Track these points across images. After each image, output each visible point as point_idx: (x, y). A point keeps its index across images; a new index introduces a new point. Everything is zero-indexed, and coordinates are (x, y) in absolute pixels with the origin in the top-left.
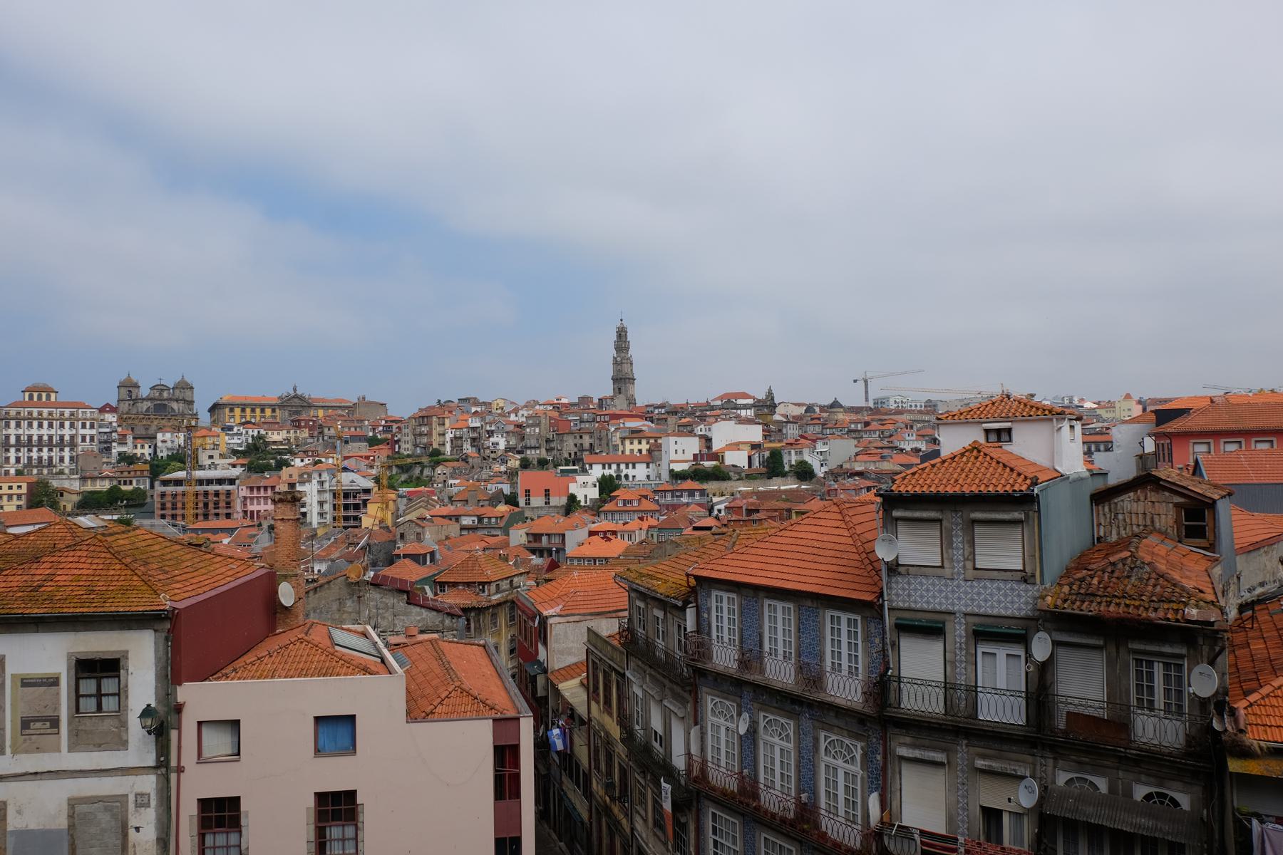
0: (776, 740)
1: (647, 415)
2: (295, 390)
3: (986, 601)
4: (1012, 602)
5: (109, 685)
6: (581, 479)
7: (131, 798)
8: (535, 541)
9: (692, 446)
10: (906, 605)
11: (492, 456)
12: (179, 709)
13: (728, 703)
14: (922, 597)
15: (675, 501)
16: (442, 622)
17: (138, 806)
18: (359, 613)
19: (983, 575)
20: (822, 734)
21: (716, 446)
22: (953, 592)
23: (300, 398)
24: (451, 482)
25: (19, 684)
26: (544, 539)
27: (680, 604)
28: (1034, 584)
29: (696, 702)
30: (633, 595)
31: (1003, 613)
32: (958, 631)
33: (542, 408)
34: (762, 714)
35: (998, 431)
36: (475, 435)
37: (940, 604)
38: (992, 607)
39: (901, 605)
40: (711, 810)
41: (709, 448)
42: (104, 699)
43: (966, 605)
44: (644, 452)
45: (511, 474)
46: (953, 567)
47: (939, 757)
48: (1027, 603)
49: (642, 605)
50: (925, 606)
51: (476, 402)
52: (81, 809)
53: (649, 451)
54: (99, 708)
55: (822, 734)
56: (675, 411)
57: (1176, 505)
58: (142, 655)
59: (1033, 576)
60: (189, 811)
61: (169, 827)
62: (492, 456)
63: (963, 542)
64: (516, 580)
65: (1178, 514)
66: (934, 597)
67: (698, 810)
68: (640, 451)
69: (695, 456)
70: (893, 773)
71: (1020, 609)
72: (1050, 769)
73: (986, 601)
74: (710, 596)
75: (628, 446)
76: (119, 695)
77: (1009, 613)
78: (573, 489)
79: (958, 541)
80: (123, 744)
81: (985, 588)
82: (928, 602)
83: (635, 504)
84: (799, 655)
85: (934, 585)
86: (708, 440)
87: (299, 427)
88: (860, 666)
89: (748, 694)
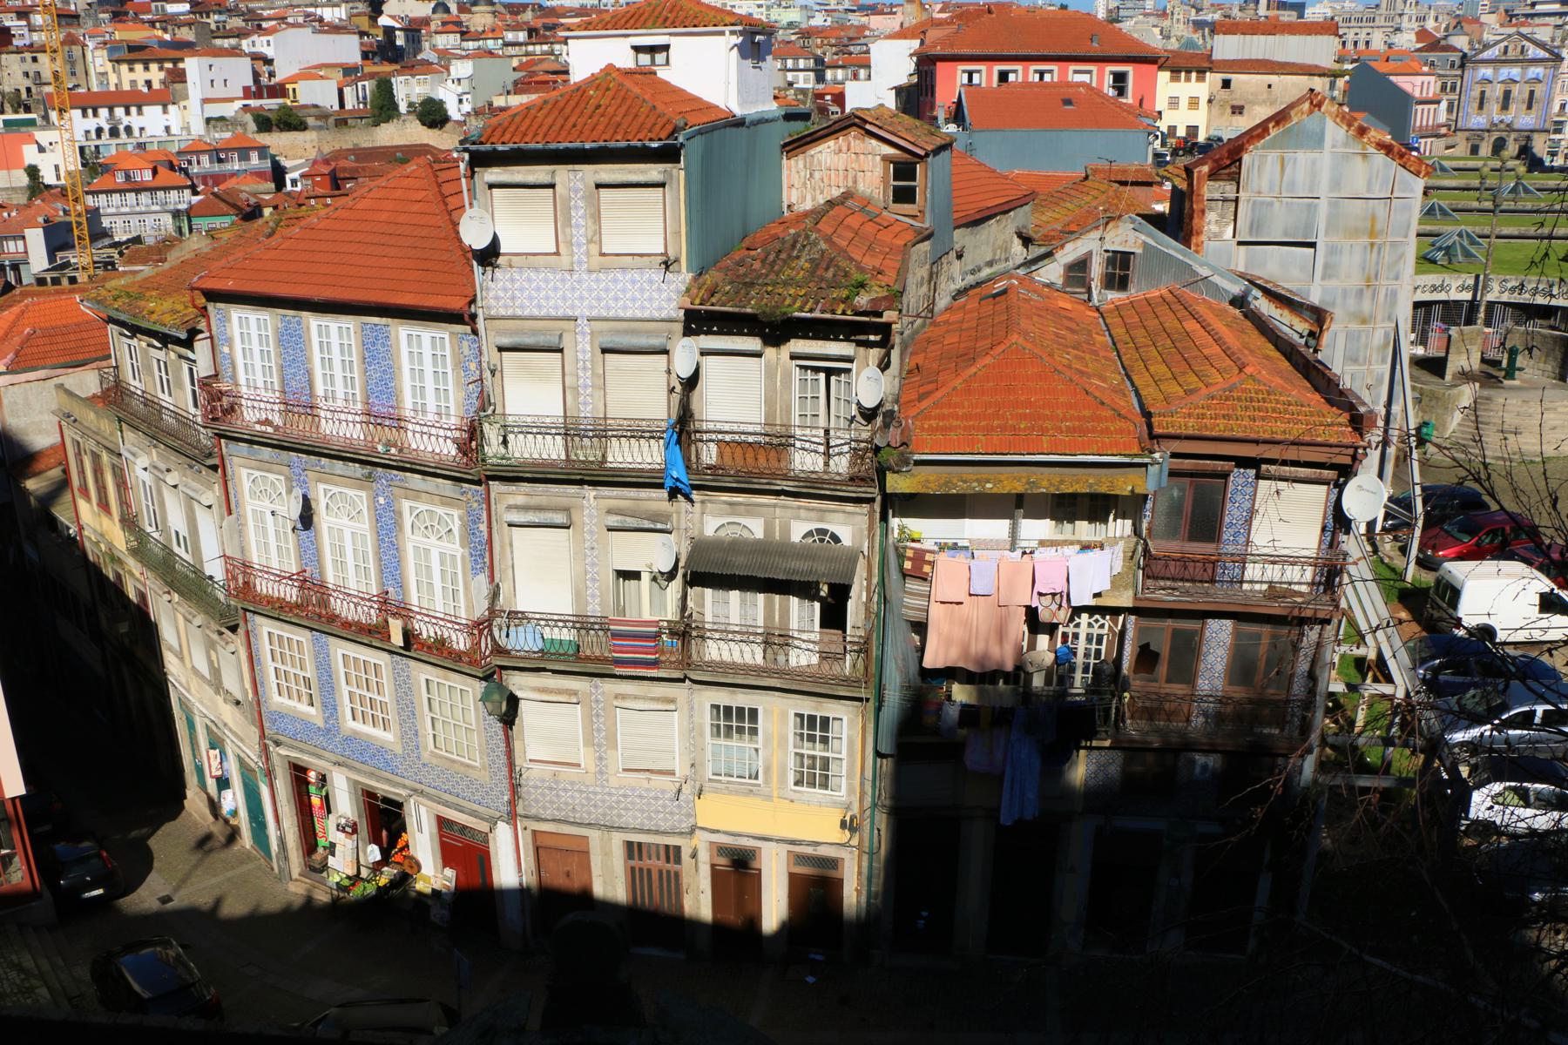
3: (616, 299)
4: (651, 299)
6: (43, 137)
9: (240, 73)
10: (510, 312)
13: (271, 476)
14: (530, 298)
15: (217, 168)
19: (609, 261)
20: (406, 505)
21: (283, 72)
22: (573, 289)
27: (183, 336)
28: (679, 272)
31: (639, 314)
32: (581, 346)
34: (321, 487)
35: (652, 50)
37: (556, 308)
38: (625, 308)
39: (502, 312)
40: (265, 630)
41: (272, 75)
43: (591, 308)
44: (156, 85)
46: (572, 254)
47: (559, 518)
48: (670, 300)
50: (536, 312)
53: (163, 82)
55: (406, 505)
57: (885, 158)
59: (677, 260)
63: (583, 217)
65: (886, 170)
66: (547, 298)
67: (247, 633)
68: (148, 83)
69: (246, 89)
70: (502, 547)
71: (660, 309)
72: (697, 516)
73: (616, 299)
77: (646, 314)
78: (30, 155)
79: (579, 215)
81: (615, 281)
82: (539, 307)
83: (148, 176)
85: (547, 281)
88: (452, 405)
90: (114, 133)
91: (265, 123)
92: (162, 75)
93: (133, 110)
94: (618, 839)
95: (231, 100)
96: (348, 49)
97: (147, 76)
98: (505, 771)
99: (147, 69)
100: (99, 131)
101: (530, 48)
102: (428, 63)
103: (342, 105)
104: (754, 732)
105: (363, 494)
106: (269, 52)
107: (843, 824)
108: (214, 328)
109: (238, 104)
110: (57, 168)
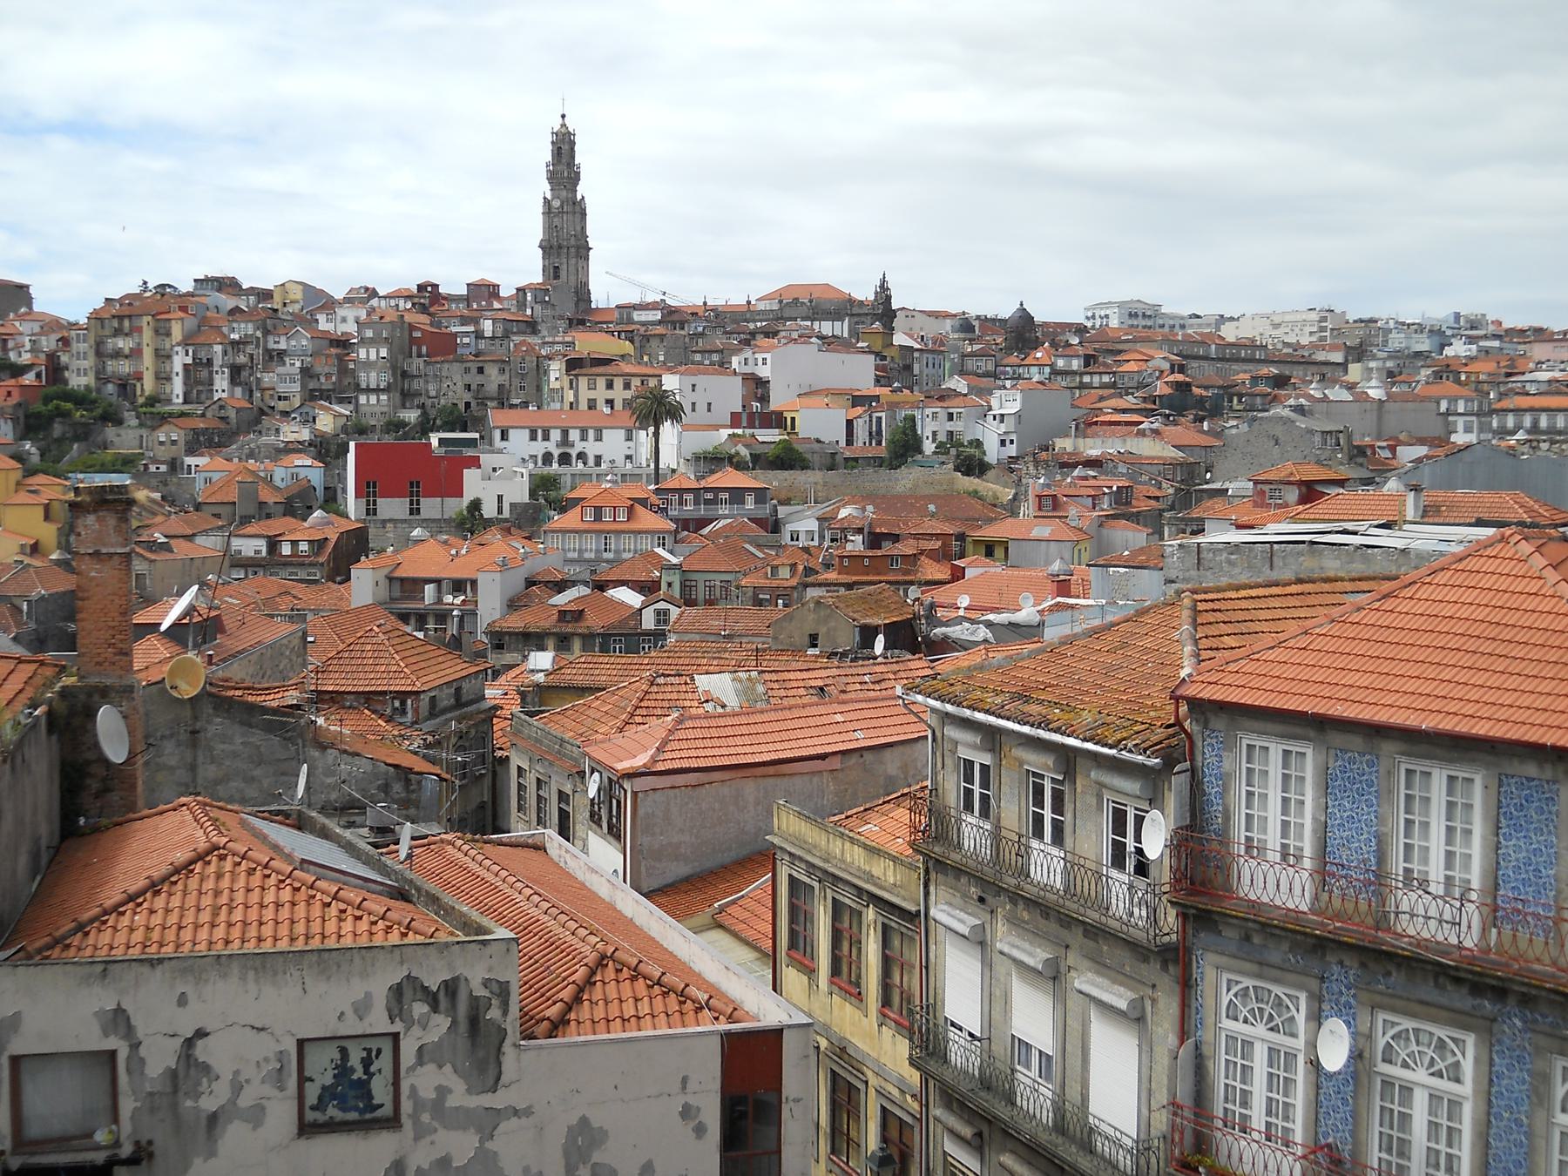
0: (1420, 1075)
1: (622, 320)
8: (407, 598)
9: (728, 394)
11: (282, 405)
13: (1278, 990)
16: (386, 788)
18: (193, 768)
24: (189, 460)
26: (429, 589)
29: (1186, 985)
30: (952, 732)
33: (383, 303)
34: (1381, 1016)
36: (242, 359)
41: (764, 399)
44: (618, 405)
45: (327, 450)
49: (982, 758)
51: (228, 285)
53: (627, 404)
56: (673, 317)
62: (282, 405)
64: (465, 685)
69: (735, 420)
74: (1229, 745)
75: (585, 394)
83: (622, 518)
84: (1494, 883)
86: (758, 387)
89: (1341, 972)
90: (565, 459)
91: (760, 461)
92: (628, 394)
93: (591, 433)
95: (717, 427)
96: (859, 372)
97: (610, 394)
99: (610, 386)
100: (547, 458)
101: (1086, 379)
102: (957, 394)
103: (849, 442)
105: (1470, 1040)
106: (764, 372)
108: (1199, 758)
109: (725, 433)
110: (500, 498)
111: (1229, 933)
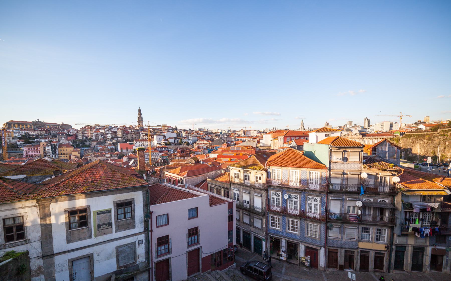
2: (38, 119)
5: (128, 209)
7: (137, 242)
12: (151, 213)
17: (139, 244)
23: (41, 122)
25: (96, 214)
29: (267, 193)
42: (126, 214)
52: (120, 250)
54: (125, 217)
58: (138, 198)
60: (155, 241)
61: (149, 248)
76: (131, 212)
80: (134, 227)
87: (42, 131)
94: (343, 250)
98: (325, 238)
104: (369, 232)
107: (386, 247)
111: (272, 187)
